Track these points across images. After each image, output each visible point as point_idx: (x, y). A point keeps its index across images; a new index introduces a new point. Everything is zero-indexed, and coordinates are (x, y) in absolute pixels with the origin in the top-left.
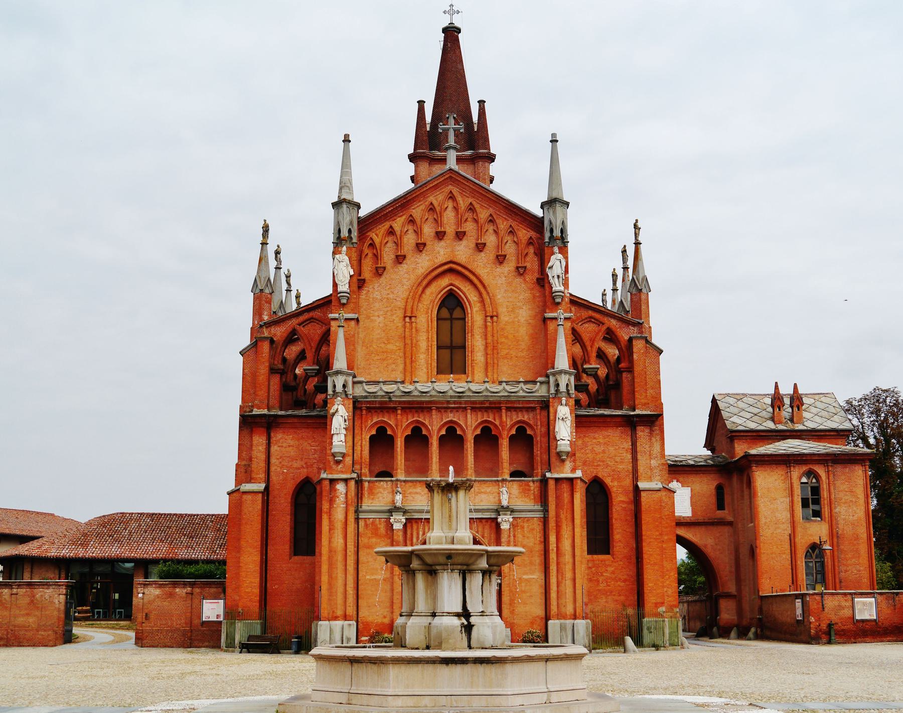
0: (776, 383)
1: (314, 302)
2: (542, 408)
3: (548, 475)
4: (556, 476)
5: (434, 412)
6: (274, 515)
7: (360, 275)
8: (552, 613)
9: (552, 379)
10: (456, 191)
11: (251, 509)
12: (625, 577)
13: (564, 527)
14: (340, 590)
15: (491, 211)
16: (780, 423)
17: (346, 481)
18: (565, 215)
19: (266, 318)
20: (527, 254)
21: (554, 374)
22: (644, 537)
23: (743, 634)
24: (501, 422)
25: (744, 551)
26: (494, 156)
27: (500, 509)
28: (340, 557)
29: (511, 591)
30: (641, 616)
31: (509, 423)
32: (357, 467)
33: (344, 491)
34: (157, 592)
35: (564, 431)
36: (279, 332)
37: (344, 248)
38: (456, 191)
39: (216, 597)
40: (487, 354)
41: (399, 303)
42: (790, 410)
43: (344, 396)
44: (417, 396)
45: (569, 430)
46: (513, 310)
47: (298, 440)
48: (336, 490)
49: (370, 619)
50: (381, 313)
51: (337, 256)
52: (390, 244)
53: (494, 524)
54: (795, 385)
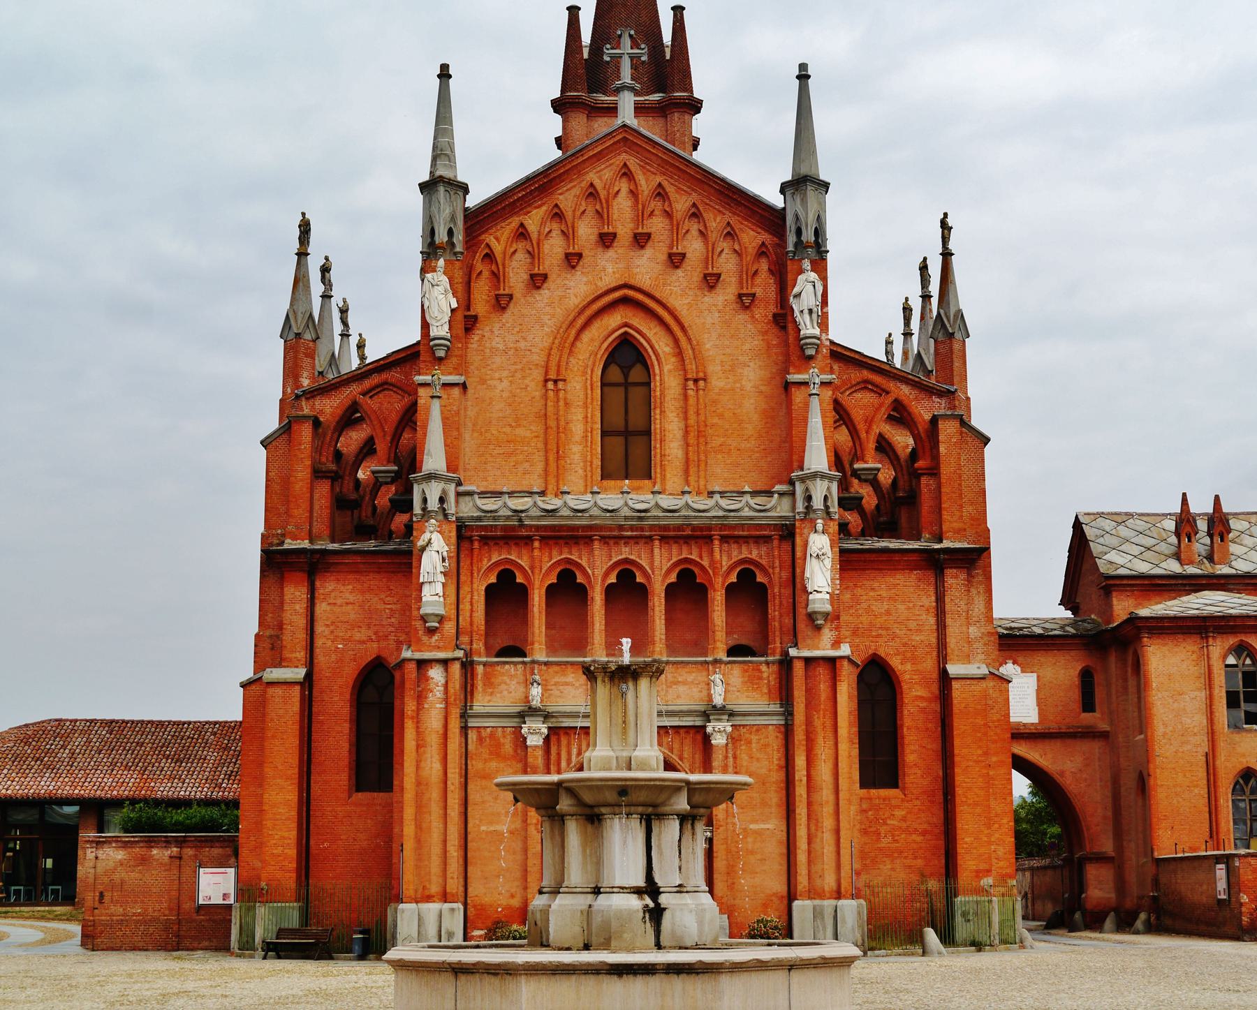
0: (1184, 495)
1: (389, 356)
2: (782, 538)
3: (793, 652)
5: (596, 545)
6: (322, 723)
7: (469, 310)
8: (800, 888)
9: (799, 488)
10: (633, 163)
11: (281, 712)
12: (925, 826)
13: (820, 740)
14: (436, 850)
15: (695, 197)
16: (1191, 563)
17: (445, 663)
18: (822, 205)
19: (306, 382)
20: (756, 273)
21: (802, 480)
22: (957, 759)
23: (1125, 924)
24: (712, 562)
25: (1129, 782)
26: (700, 102)
27: (711, 711)
28: (435, 794)
29: (728, 851)
30: (951, 893)
31: (726, 563)
32: (464, 639)
33: (443, 681)
34: (120, 855)
35: (820, 577)
36: (328, 407)
37: (441, 262)
38: (633, 163)
39: (221, 863)
40: (688, 445)
41: (535, 357)
42: (1207, 540)
43: (441, 517)
44: (568, 517)
45: (828, 575)
46: (732, 369)
47: (363, 592)
48: (427, 679)
49: (487, 900)
50: (505, 373)
51: (429, 276)
52: (521, 256)
53: (699, 737)
54: (1217, 498)
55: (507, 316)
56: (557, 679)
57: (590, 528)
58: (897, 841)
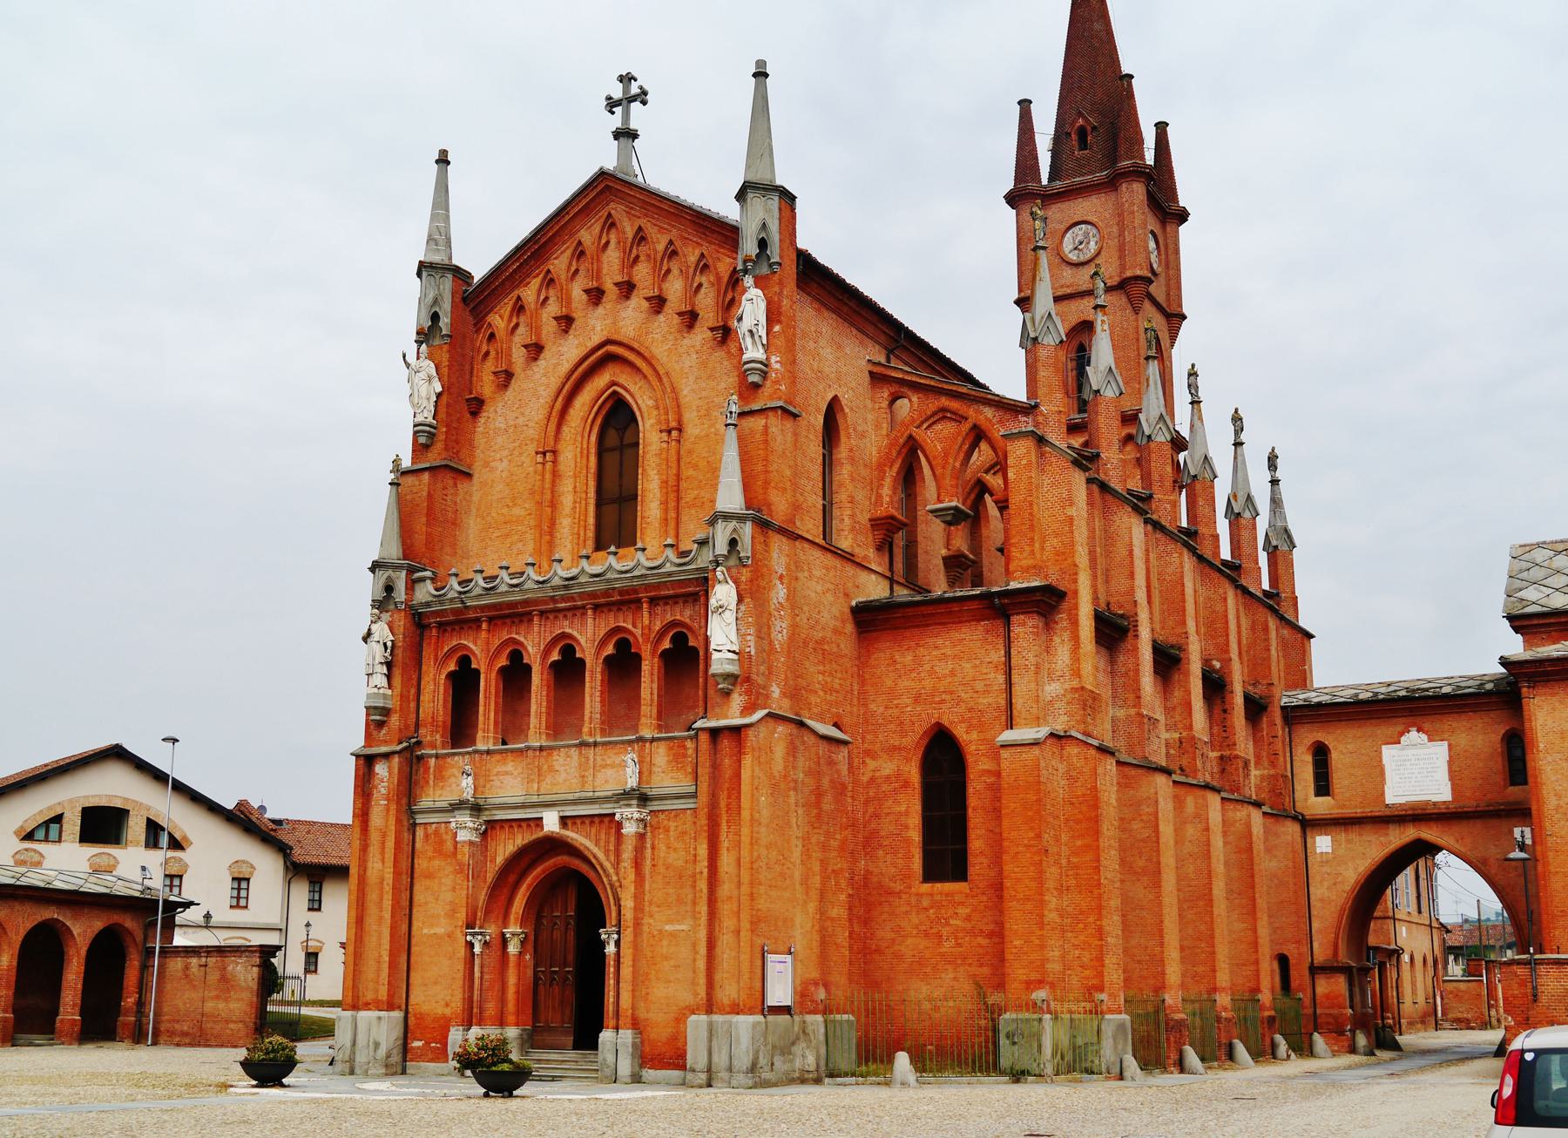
4: (713, 724)
12: (991, 927)
17: (386, 756)
23: (1219, 1054)
31: (658, 626)
49: (425, 1008)
50: (506, 453)
55: (510, 393)
56: (498, 769)
57: (526, 602)
58: (959, 945)
